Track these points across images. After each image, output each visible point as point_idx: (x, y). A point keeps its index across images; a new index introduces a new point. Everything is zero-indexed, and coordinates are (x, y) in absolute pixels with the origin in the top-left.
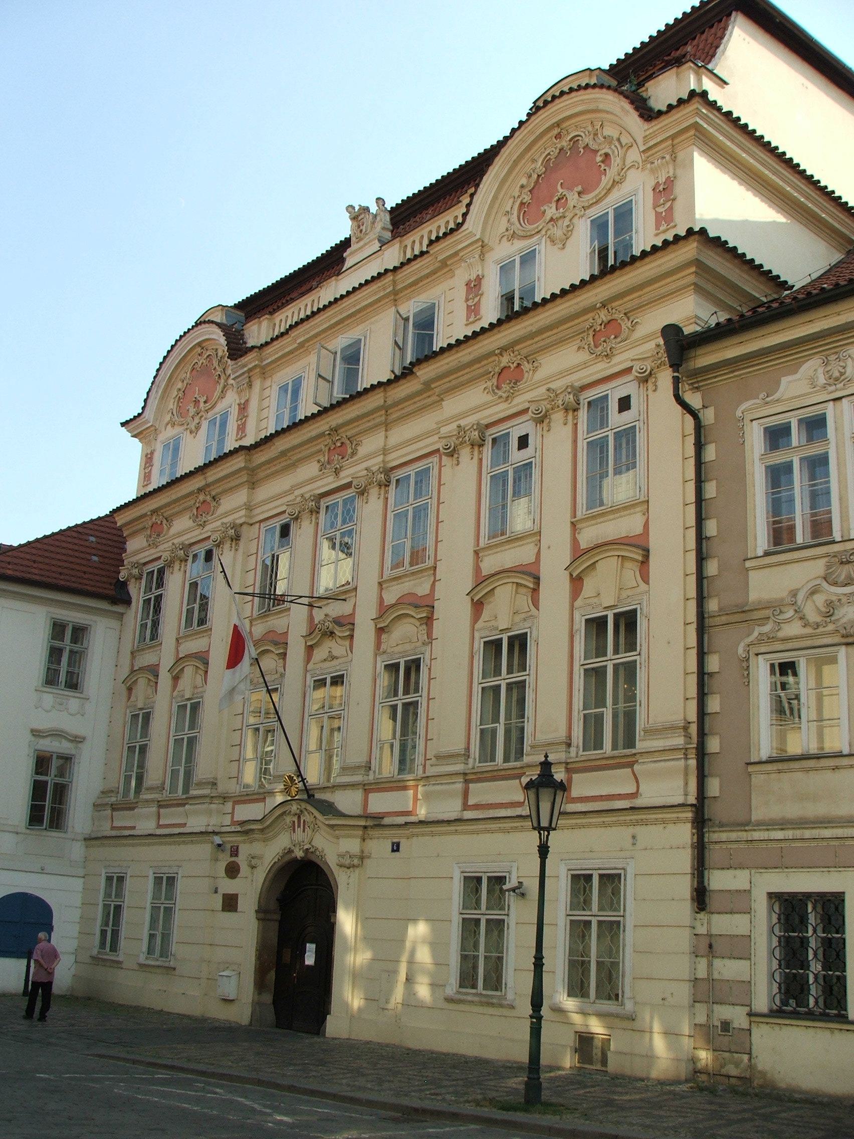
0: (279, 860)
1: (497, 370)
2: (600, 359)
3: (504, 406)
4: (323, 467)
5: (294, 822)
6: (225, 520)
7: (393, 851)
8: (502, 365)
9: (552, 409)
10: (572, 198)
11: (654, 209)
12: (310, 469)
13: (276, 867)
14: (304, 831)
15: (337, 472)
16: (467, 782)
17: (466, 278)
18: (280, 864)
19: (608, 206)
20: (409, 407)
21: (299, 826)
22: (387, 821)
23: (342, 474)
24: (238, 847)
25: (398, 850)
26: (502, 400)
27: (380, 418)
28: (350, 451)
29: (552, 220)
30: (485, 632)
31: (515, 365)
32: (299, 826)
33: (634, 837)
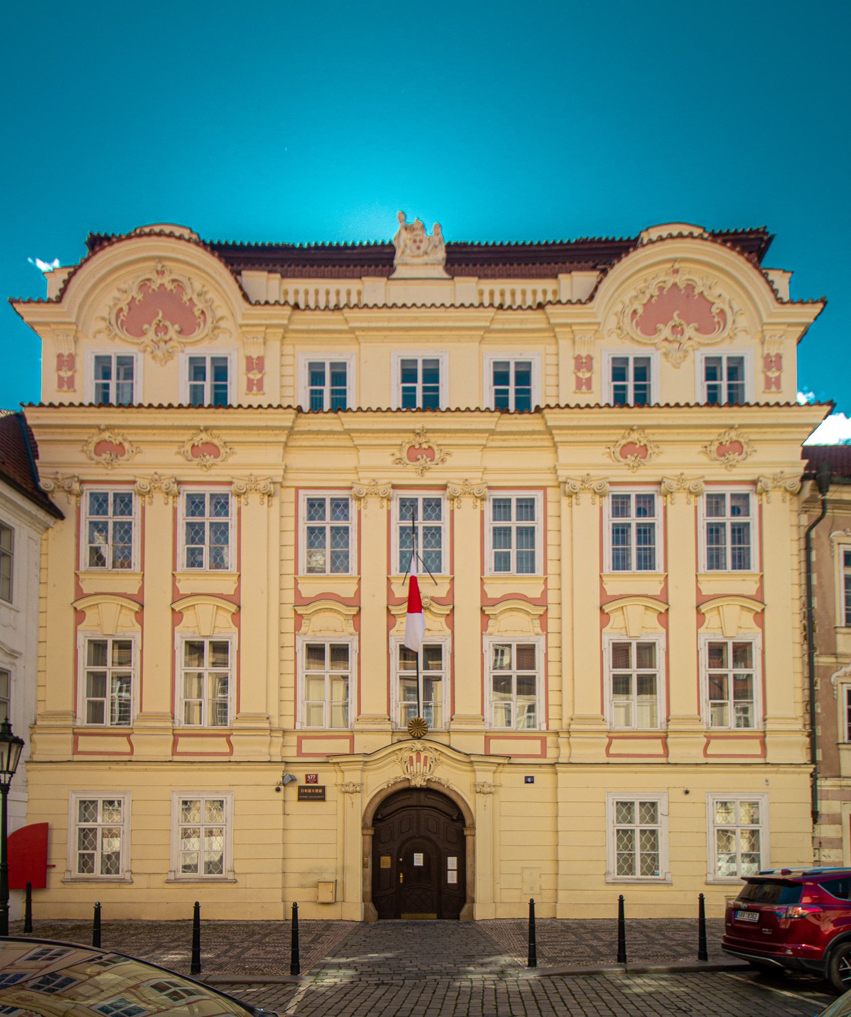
0: (388, 786)
1: (624, 442)
2: (723, 466)
3: (629, 472)
4: (399, 461)
5: (411, 758)
6: (255, 472)
7: (527, 782)
8: (630, 440)
9: (679, 489)
10: (690, 331)
11: (764, 372)
12: (384, 458)
13: (384, 795)
14: (425, 764)
15: (424, 469)
16: (611, 738)
17: (577, 353)
18: (390, 791)
19: (724, 350)
20: (512, 442)
21: (418, 760)
22: (513, 760)
23: (427, 474)
24: (317, 776)
26: (627, 467)
27: (482, 440)
28: (437, 456)
29: (666, 339)
30: (614, 634)
31: (642, 444)
32: (418, 760)
33: (767, 781)
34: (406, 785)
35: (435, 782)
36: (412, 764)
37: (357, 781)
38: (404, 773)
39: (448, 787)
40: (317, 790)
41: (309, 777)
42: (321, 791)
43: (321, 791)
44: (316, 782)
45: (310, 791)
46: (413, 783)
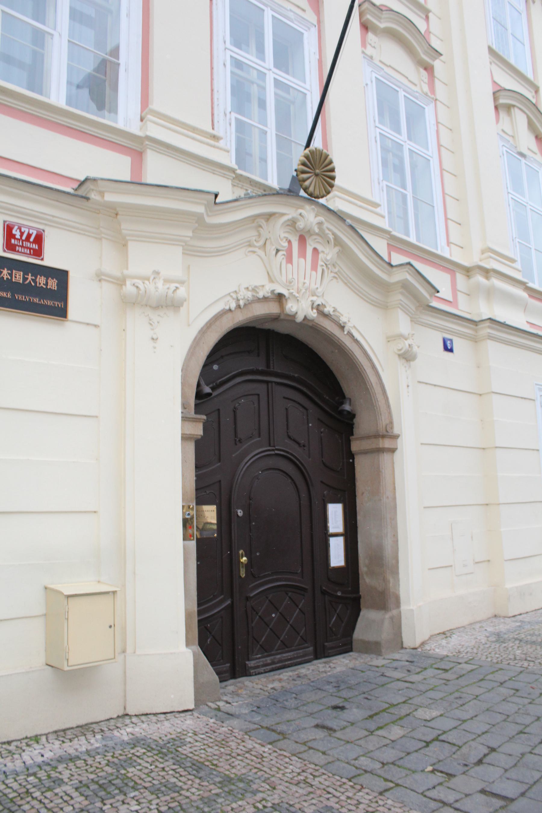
0: (239, 307)
14: (314, 267)
21: (302, 254)
25: (451, 350)
32: (302, 254)
34: (272, 309)
35: (326, 316)
36: (289, 259)
37: (177, 272)
38: (271, 280)
39: (350, 334)
40: (41, 280)
41: (16, 232)
42: (53, 284)
43: (53, 284)
44: (38, 253)
45: (18, 277)
46: (291, 307)
